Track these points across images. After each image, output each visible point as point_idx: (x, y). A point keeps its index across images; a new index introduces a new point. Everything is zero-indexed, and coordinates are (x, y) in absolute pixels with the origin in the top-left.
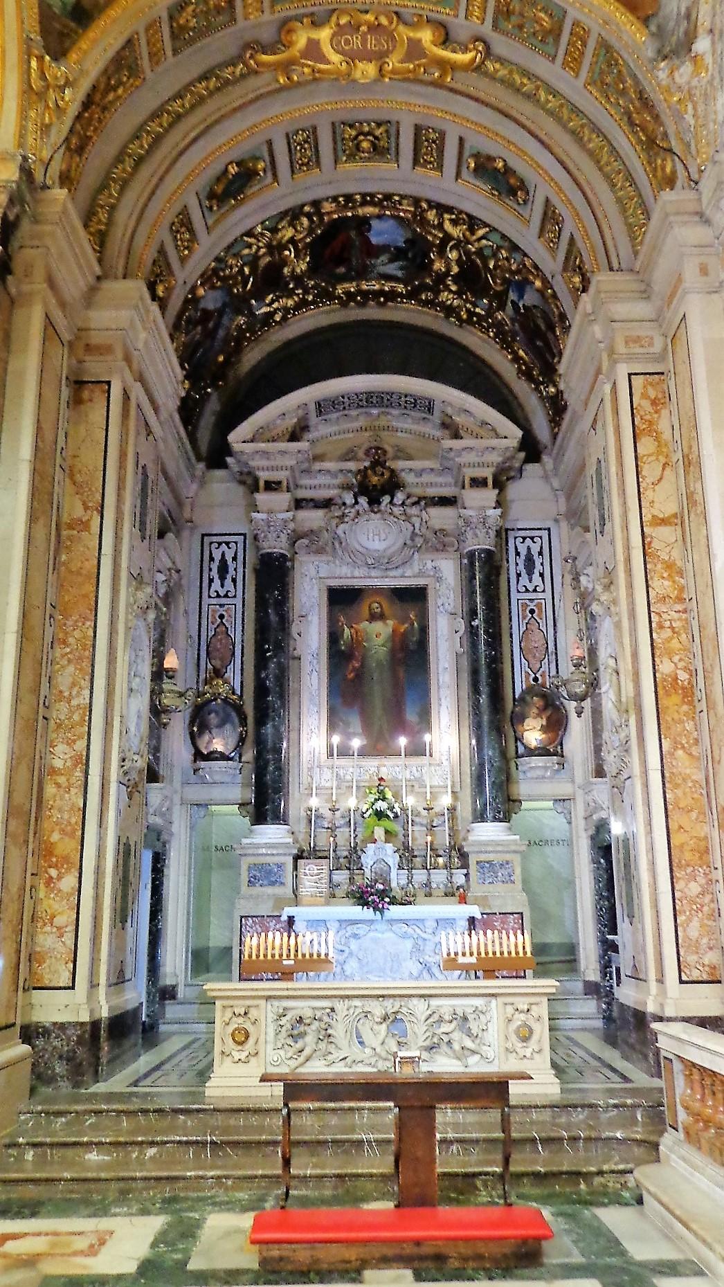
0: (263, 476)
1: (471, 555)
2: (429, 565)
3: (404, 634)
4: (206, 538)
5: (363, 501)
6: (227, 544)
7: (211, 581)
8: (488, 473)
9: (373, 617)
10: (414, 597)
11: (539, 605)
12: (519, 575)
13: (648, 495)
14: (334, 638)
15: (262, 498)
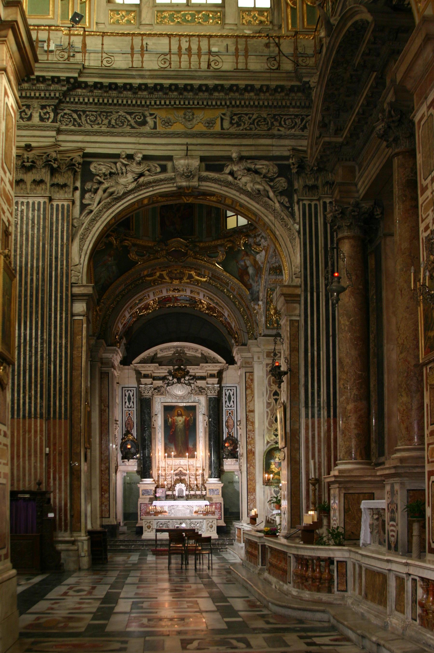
0: (143, 372)
1: (210, 398)
2: (197, 399)
3: (188, 421)
4: (124, 389)
5: (175, 380)
6: (131, 390)
7: (126, 402)
8: (215, 372)
9: (179, 415)
10: (192, 410)
11: (232, 412)
12: (226, 402)
13: (248, 404)
14: (166, 421)
15: (143, 380)
